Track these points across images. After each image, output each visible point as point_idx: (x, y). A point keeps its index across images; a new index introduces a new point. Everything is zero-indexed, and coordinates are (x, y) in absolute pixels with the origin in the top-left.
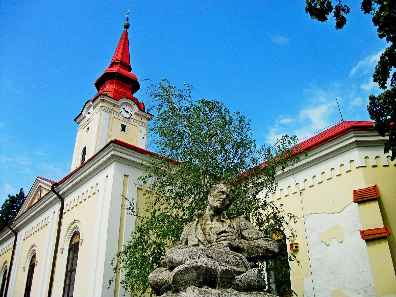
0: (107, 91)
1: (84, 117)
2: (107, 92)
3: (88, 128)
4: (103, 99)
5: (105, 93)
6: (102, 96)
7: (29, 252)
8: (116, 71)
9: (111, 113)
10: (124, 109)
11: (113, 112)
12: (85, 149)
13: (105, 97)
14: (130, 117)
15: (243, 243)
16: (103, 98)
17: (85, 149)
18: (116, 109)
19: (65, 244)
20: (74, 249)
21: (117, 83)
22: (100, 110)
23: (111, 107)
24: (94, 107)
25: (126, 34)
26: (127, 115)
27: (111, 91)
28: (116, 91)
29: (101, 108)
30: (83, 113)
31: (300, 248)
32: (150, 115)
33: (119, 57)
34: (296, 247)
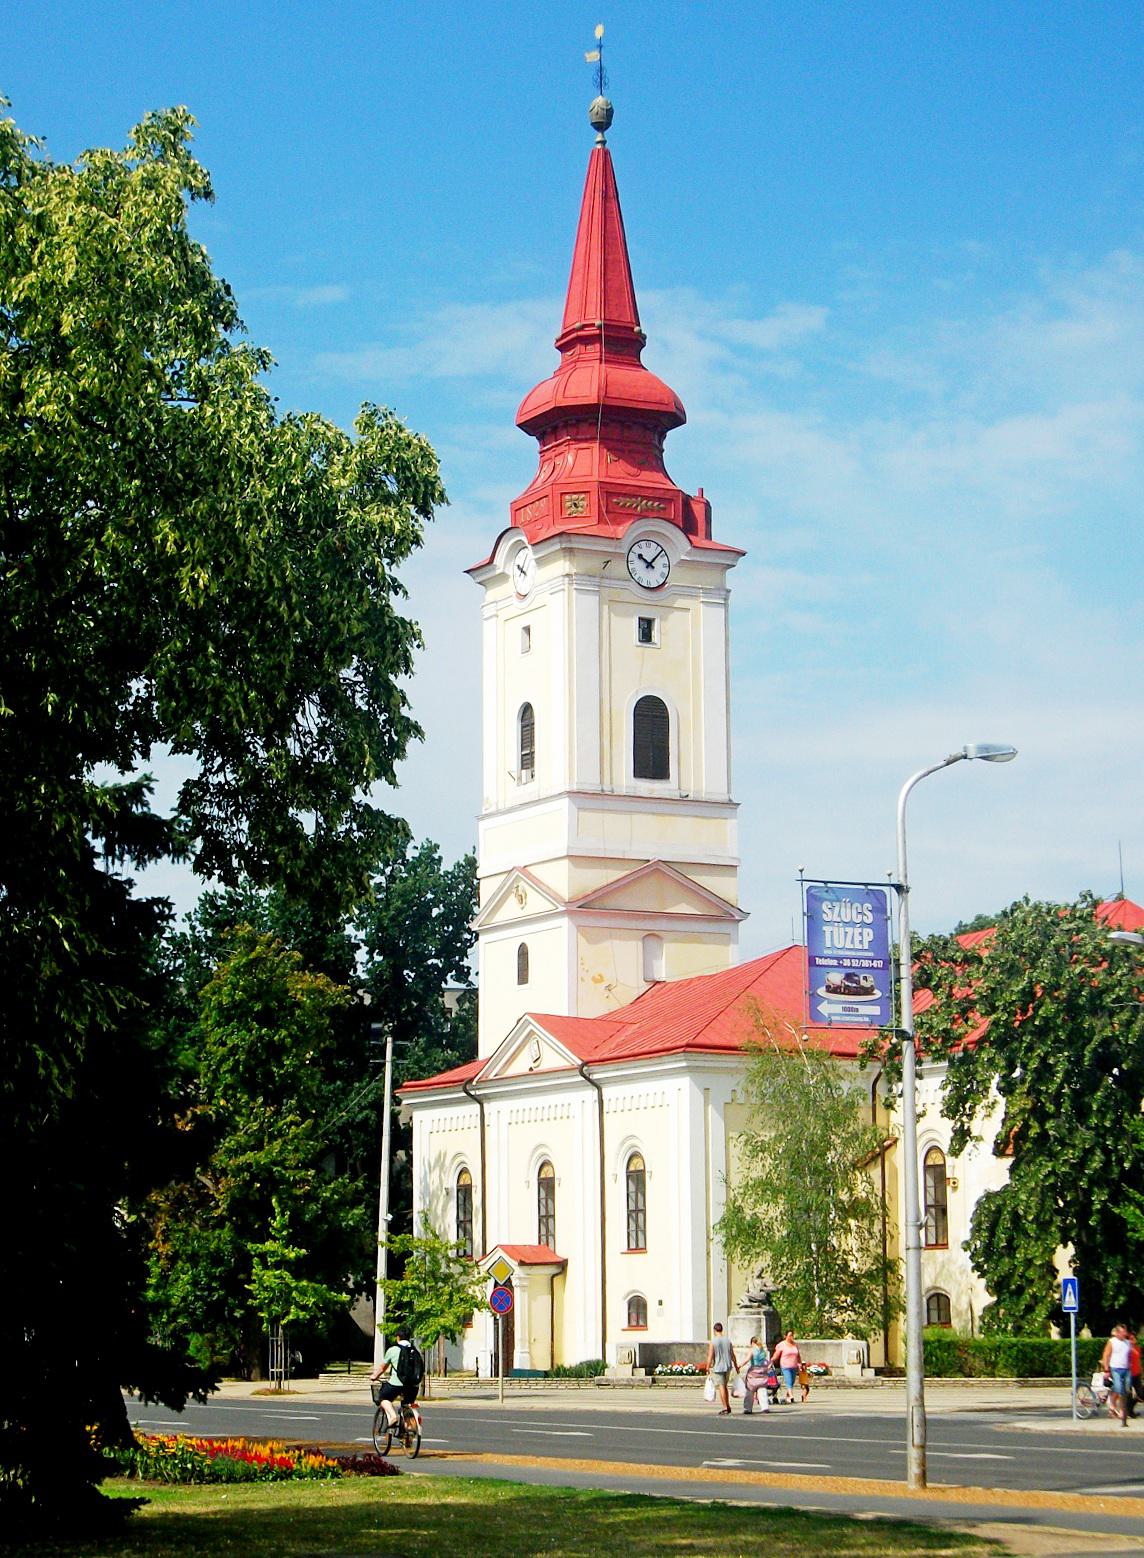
0: (575, 493)
1: (503, 577)
2: (575, 496)
3: (527, 630)
4: (569, 545)
5: (567, 497)
6: (564, 537)
7: (532, 1156)
8: (593, 400)
9: (602, 589)
10: (640, 556)
11: (608, 581)
12: (527, 709)
13: (573, 538)
17: (527, 709)
18: (618, 568)
19: (617, 1169)
20: (637, 1179)
21: (605, 442)
22: (566, 587)
23: (596, 563)
24: (540, 562)
25: (605, 162)
26: (653, 578)
29: (567, 579)
31: (960, 1184)
32: (733, 555)
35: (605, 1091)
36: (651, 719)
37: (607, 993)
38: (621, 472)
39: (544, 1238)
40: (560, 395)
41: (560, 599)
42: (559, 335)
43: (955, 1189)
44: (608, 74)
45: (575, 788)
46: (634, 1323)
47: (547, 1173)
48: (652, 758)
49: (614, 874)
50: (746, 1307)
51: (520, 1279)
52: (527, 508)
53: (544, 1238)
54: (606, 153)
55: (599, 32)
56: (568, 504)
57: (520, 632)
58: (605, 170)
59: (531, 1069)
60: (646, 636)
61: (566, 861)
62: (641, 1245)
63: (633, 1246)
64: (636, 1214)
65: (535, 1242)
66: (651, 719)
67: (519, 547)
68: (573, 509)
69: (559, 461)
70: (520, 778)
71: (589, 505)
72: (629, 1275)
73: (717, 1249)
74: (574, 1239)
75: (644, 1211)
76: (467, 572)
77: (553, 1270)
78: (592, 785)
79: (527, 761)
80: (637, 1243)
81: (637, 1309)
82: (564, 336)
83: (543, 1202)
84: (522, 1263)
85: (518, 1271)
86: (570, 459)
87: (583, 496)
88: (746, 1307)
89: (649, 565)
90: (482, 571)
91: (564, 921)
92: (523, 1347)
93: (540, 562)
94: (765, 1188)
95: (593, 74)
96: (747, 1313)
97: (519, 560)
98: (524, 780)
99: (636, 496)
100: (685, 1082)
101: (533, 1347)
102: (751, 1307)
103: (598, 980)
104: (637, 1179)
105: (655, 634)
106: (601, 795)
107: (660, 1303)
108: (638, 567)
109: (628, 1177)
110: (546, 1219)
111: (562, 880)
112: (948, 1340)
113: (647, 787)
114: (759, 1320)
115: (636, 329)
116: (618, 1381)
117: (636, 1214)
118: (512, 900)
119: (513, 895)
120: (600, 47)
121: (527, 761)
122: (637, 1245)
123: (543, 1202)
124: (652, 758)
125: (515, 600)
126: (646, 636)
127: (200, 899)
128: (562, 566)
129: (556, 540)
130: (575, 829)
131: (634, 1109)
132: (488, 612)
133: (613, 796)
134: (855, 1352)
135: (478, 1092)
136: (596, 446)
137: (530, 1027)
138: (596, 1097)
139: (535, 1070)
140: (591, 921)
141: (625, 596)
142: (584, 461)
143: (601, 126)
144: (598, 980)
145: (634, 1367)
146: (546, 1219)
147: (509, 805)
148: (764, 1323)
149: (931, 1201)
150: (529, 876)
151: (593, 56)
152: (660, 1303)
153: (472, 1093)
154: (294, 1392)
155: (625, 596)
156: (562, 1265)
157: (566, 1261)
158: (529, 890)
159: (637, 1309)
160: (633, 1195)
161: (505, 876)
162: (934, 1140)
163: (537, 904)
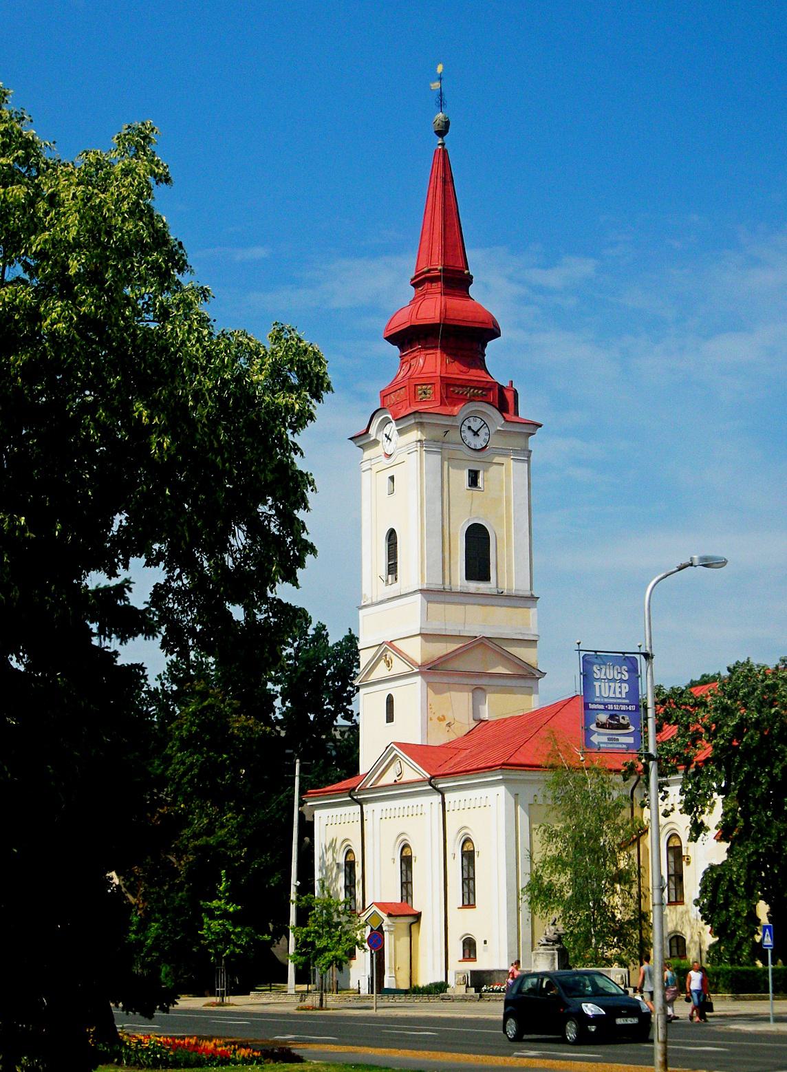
1: (376, 442)
2: (424, 387)
3: (392, 478)
4: (421, 420)
5: (419, 387)
6: (417, 415)
10: (469, 428)
11: (447, 445)
12: (392, 535)
14: (486, 446)
15: (557, 932)
16: (421, 418)
17: (392, 535)
18: (454, 436)
19: (455, 849)
20: (469, 857)
21: (445, 350)
22: (418, 449)
23: (439, 433)
24: (401, 432)
26: (478, 443)
27: (434, 384)
28: (447, 383)
29: (419, 443)
30: (373, 431)
31: (692, 860)
32: (532, 427)
33: (436, 256)
34: (688, 859)
35: (446, 796)
36: (478, 539)
37: (448, 728)
38: (456, 370)
39: (405, 898)
40: (414, 317)
41: (415, 456)
42: (413, 275)
43: (688, 863)
44: (446, 97)
45: (425, 587)
46: (467, 956)
47: (407, 852)
48: (478, 566)
49: (452, 647)
50: (544, 945)
51: (388, 926)
52: (392, 395)
53: (405, 898)
54: (445, 152)
55: (440, 68)
56: (420, 392)
57: (387, 480)
58: (444, 164)
59: (395, 781)
60: (473, 481)
61: (420, 637)
62: (472, 903)
63: (466, 903)
64: (468, 881)
65: (400, 901)
66: (478, 539)
67: (386, 422)
68: (423, 395)
69: (413, 362)
70: (387, 581)
71: (434, 392)
72: (463, 923)
73: (524, 906)
74: (426, 898)
75: (474, 879)
76: (351, 439)
77: (411, 920)
78: (436, 583)
79: (392, 569)
80: (469, 901)
81: (469, 946)
82: (416, 277)
83: (404, 872)
84: (390, 915)
85: (387, 920)
86: (421, 361)
87: (430, 386)
88: (544, 945)
89: (476, 434)
90: (362, 439)
91: (418, 679)
92: (391, 972)
93: (401, 432)
94: (558, 863)
95: (436, 97)
96: (545, 949)
97: (386, 431)
98: (390, 582)
99: (467, 387)
100: (501, 789)
101: (398, 974)
102: (547, 945)
103: (441, 719)
104: (469, 857)
105: (480, 481)
106: (442, 592)
107: (485, 942)
108: (468, 435)
109: (462, 856)
110: (406, 884)
111: (416, 650)
112: (684, 967)
113: (474, 586)
114: (554, 954)
115: (466, 272)
116: (456, 996)
117: (468, 881)
118: (382, 664)
119: (383, 661)
120: (440, 79)
121: (392, 569)
122: (469, 902)
123: (404, 872)
124: (478, 566)
125: (383, 458)
126: (473, 481)
127: (167, 664)
128: (416, 435)
129: (412, 416)
130: (426, 615)
131: (466, 809)
132: (365, 466)
133: (451, 592)
134: (620, 976)
135: (359, 797)
136: (439, 351)
137: (395, 752)
138: (440, 800)
139: (398, 781)
140: (436, 679)
141: (459, 455)
142: (431, 362)
143: (441, 133)
144: (441, 719)
145: (467, 987)
146: (406, 884)
147: (380, 599)
148: (556, 956)
149: (672, 872)
150: (394, 648)
151: (436, 85)
152: (485, 942)
153: (355, 797)
154: (233, 1005)
155: (459, 455)
156: (418, 917)
157: (421, 913)
158: (394, 657)
159: (469, 946)
160: (466, 868)
161: (377, 648)
162: (675, 829)
163: (399, 667)
